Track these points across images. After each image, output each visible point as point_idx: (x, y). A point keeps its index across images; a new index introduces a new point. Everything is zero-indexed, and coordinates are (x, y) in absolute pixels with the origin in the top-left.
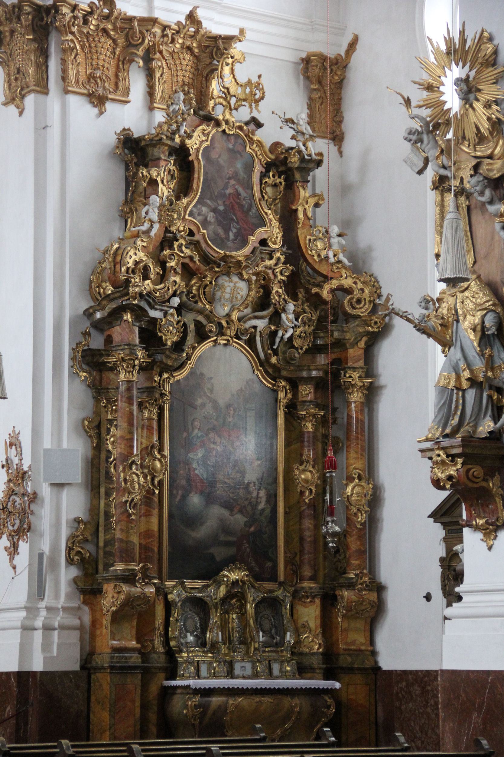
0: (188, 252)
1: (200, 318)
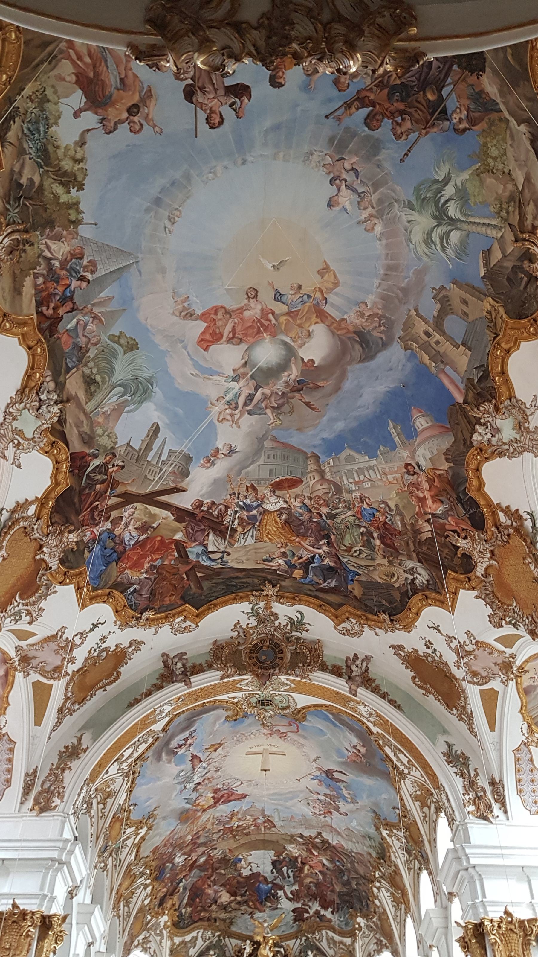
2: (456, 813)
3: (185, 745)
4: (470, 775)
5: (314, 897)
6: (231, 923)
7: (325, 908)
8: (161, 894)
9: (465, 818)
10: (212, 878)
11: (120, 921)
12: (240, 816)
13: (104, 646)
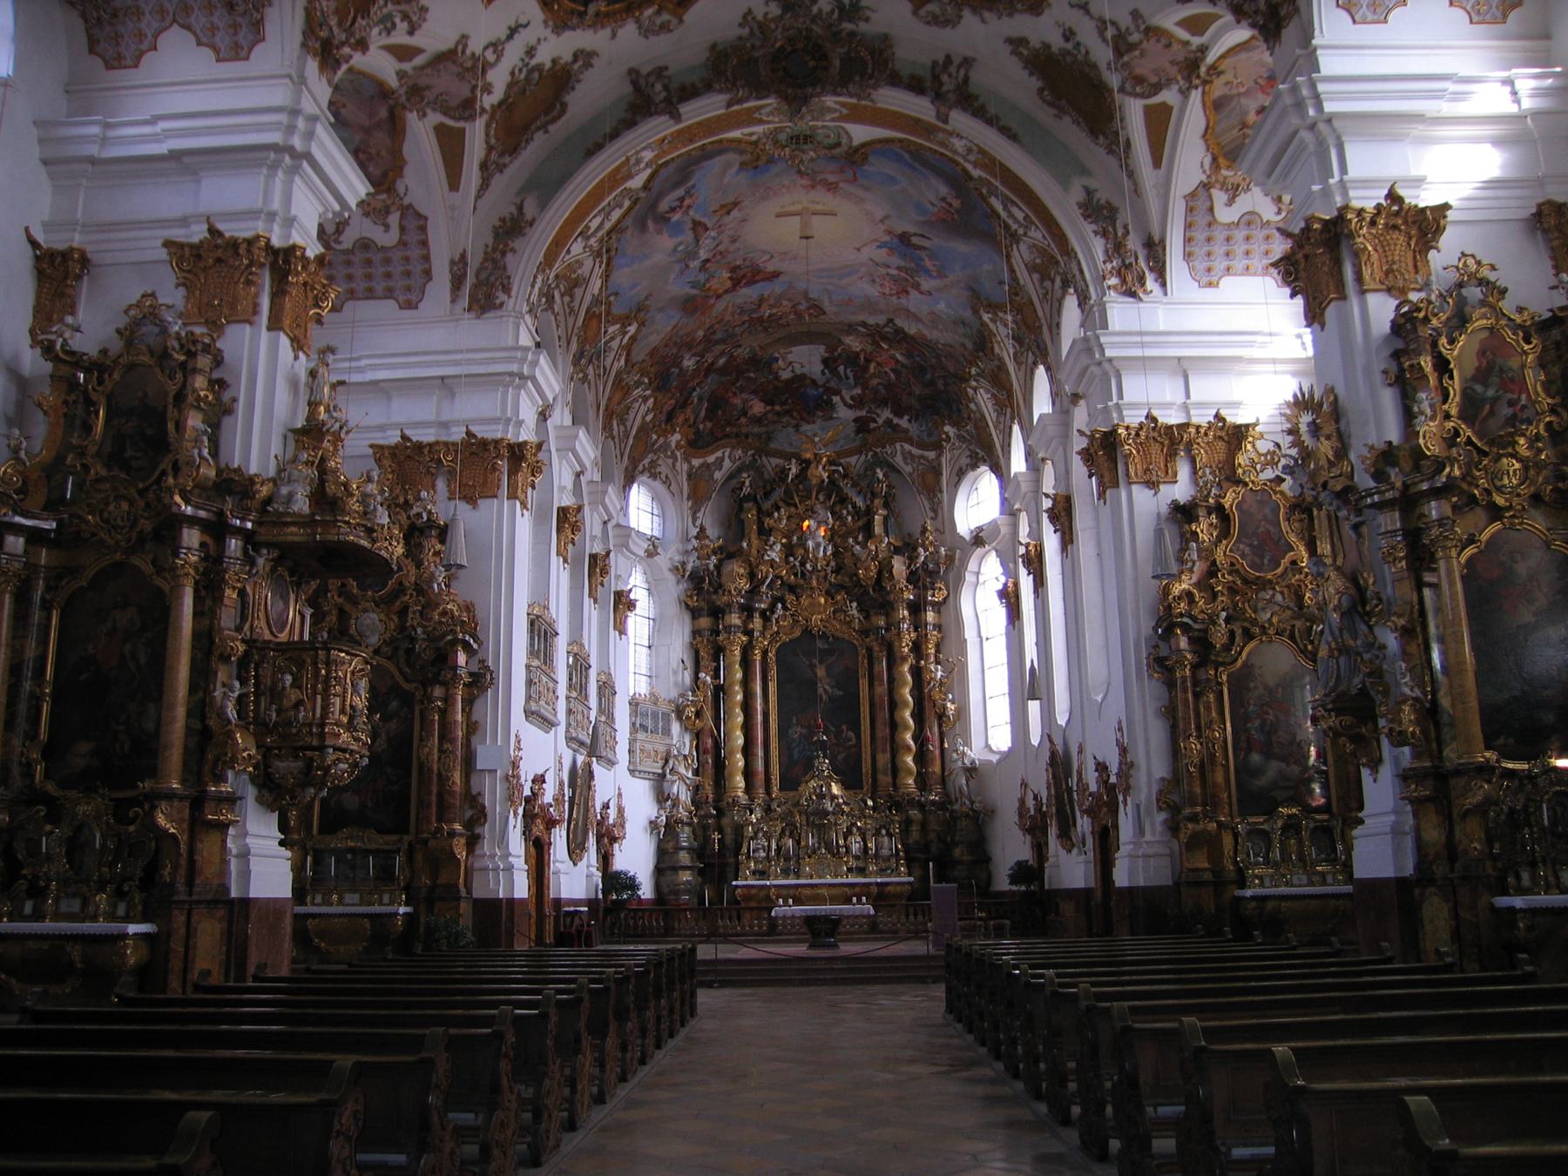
0: (1230, 578)
1: (1245, 624)
2: (1092, 289)
3: (681, 207)
4: (1116, 234)
5: (883, 403)
6: (769, 439)
7: (900, 416)
8: (667, 408)
10: (738, 384)
12: (771, 302)
13: (534, 62)
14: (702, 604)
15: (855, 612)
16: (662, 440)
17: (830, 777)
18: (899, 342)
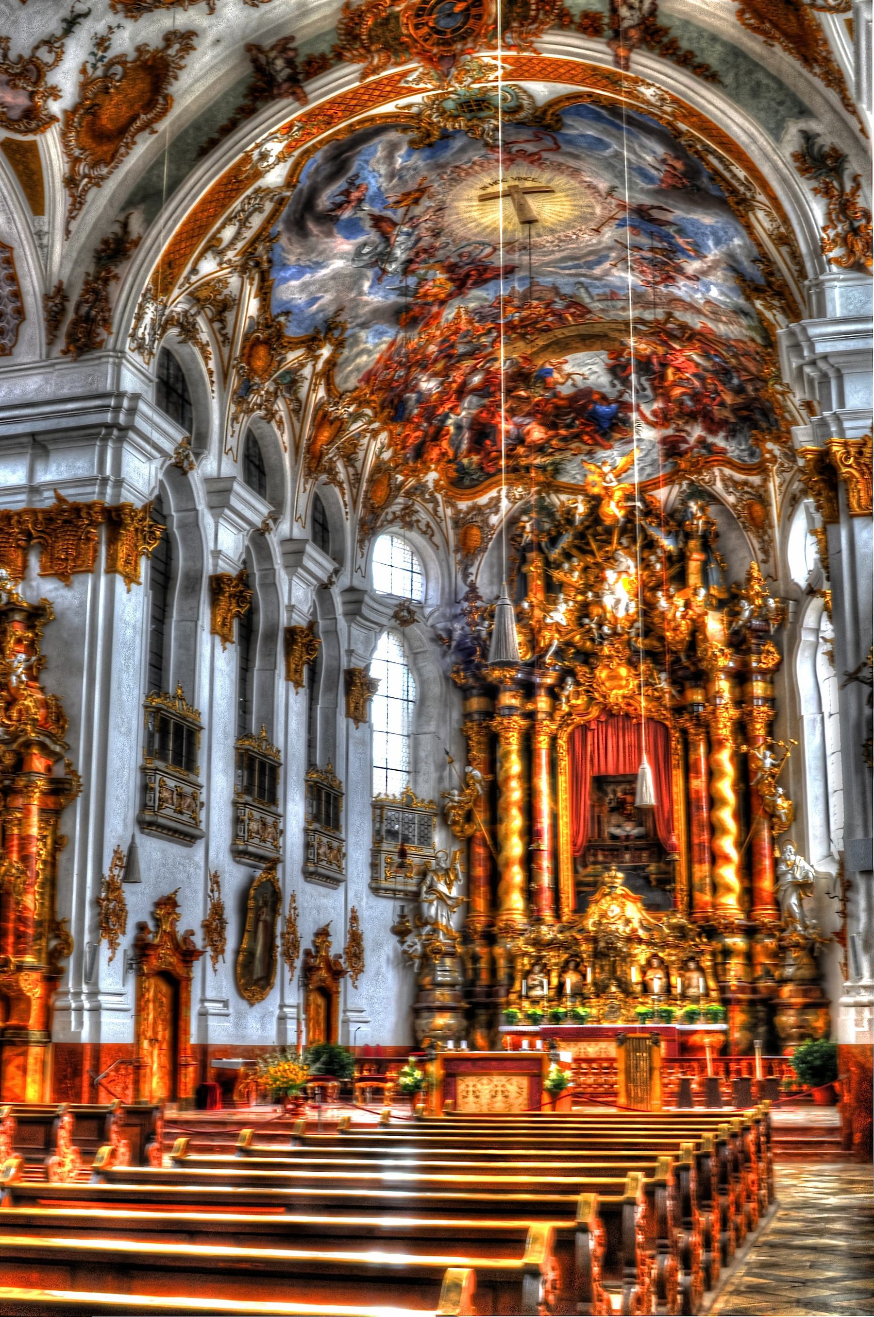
2: (808, 266)
3: (349, 202)
4: (842, 190)
5: (692, 417)
7: (713, 432)
9: (823, 271)
11: (342, 489)
14: (471, 681)
15: (664, 685)
16: (412, 482)
17: (624, 896)
18: (690, 339)
